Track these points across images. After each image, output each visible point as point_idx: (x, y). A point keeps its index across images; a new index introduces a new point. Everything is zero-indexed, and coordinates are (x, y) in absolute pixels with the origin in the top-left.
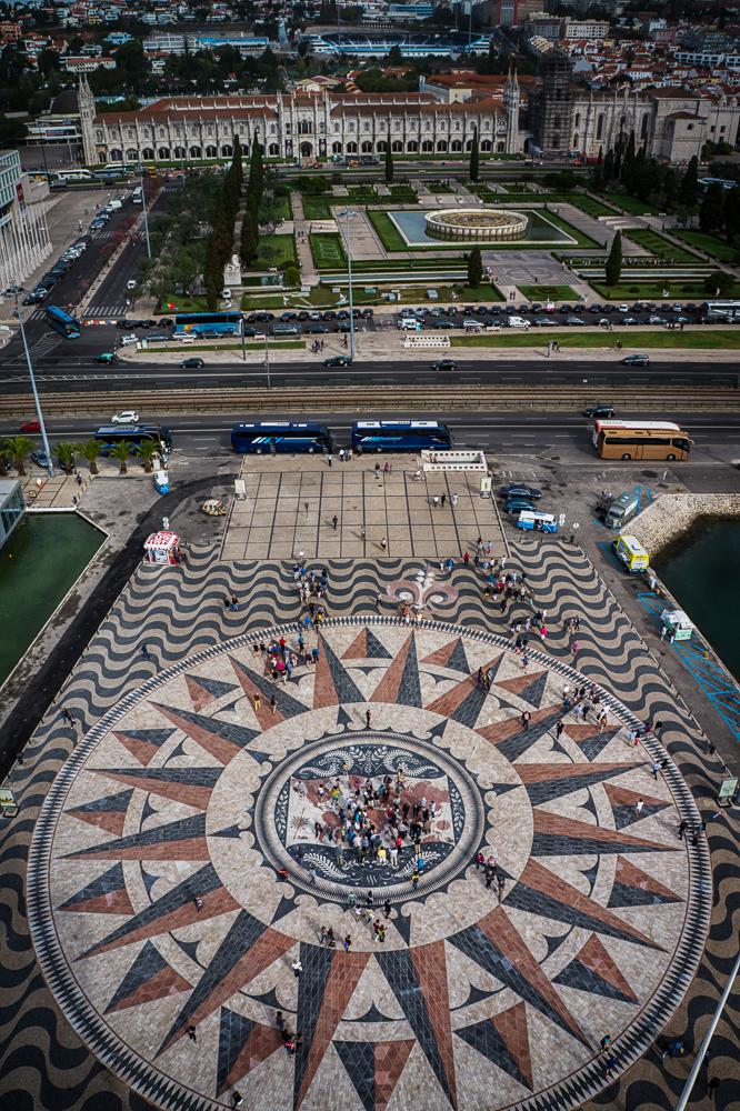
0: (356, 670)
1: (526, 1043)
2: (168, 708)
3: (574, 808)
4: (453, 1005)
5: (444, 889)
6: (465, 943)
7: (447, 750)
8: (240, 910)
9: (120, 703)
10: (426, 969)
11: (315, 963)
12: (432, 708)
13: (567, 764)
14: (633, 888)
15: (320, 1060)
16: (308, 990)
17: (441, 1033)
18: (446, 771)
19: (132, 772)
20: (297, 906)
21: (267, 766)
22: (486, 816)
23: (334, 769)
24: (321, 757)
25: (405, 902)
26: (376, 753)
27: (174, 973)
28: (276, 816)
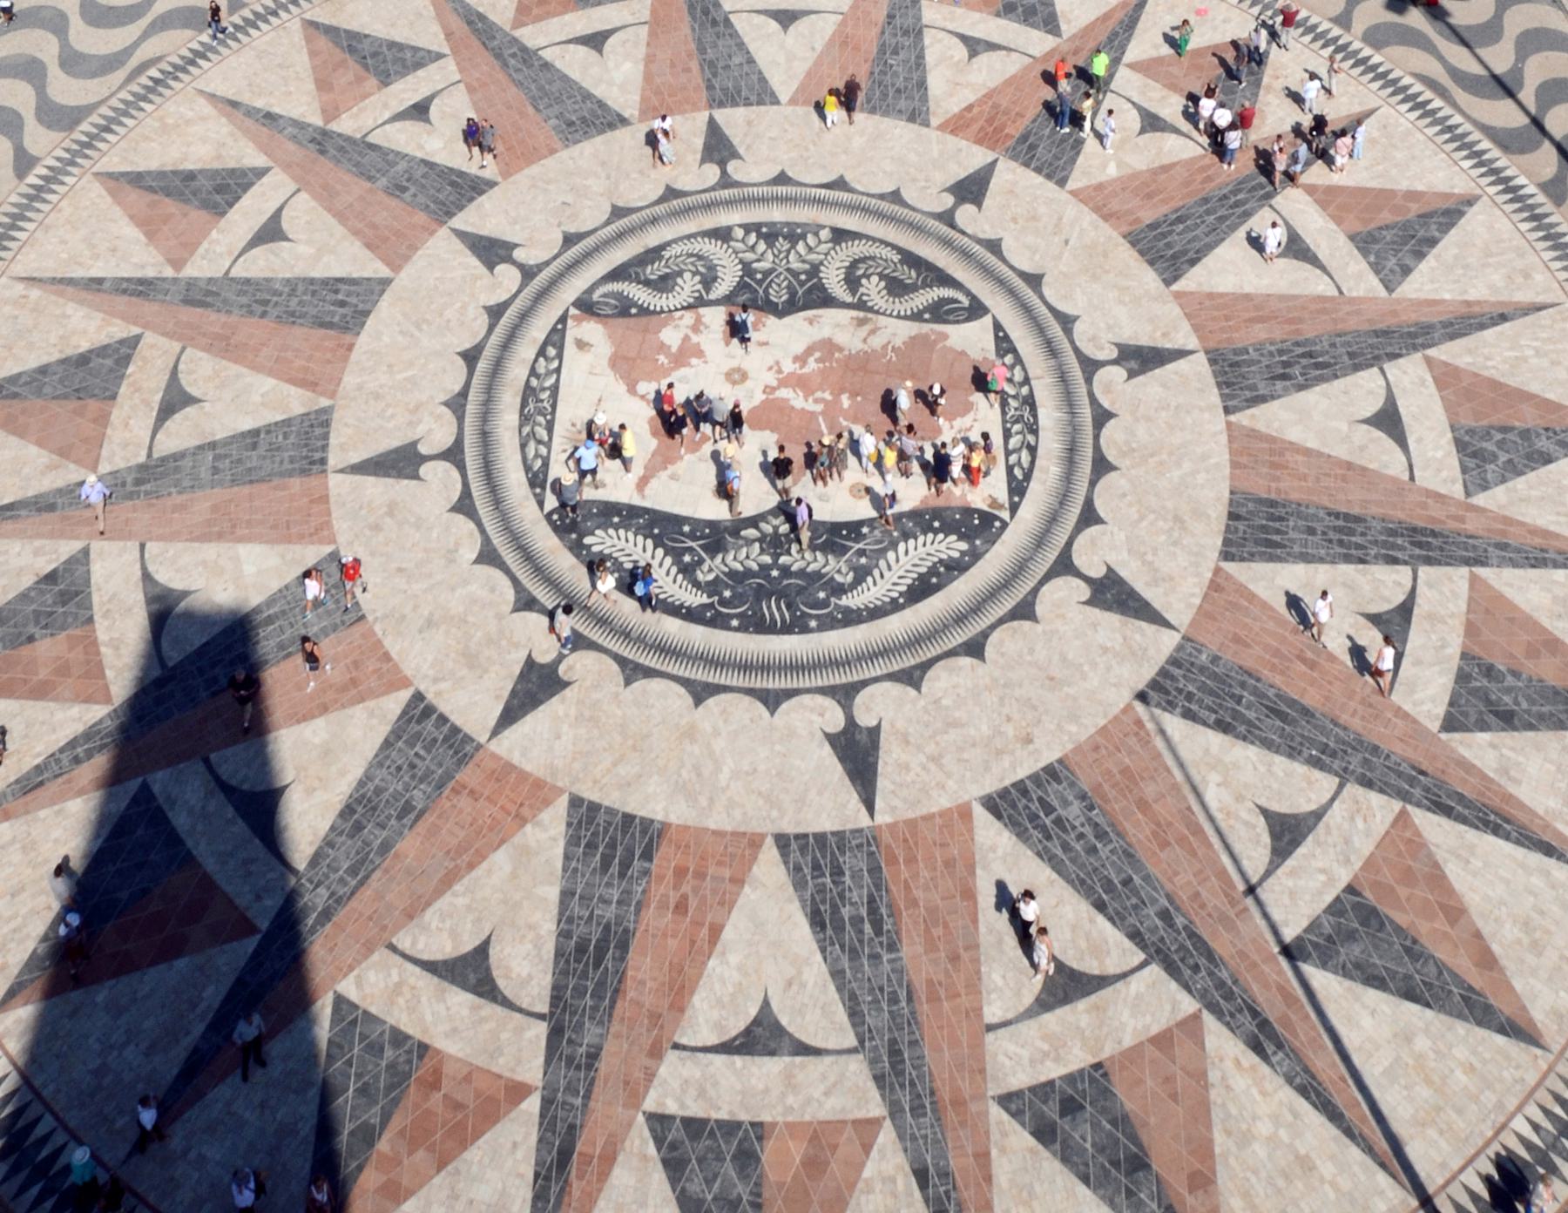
0: (763, 18)
1: (1205, 1151)
2: (250, 112)
3: (1344, 427)
4: (992, 1013)
5: (975, 648)
6: (1033, 818)
7: (994, 246)
8: (405, 695)
9: (123, 95)
10: (918, 894)
11: (606, 864)
12: (956, 126)
13: (1322, 299)
14: (1516, 674)
15: (604, 1175)
16: (581, 949)
17: (959, 1103)
18: (987, 300)
19: (142, 288)
20: (566, 684)
21: (508, 277)
22: (1097, 437)
23: (688, 286)
24: (654, 254)
25: (864, 684)
26: (801, 247)
27: (207, 884)
28: (525, 418)
